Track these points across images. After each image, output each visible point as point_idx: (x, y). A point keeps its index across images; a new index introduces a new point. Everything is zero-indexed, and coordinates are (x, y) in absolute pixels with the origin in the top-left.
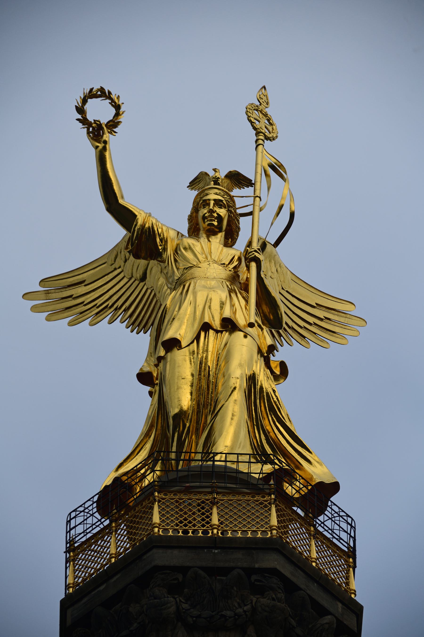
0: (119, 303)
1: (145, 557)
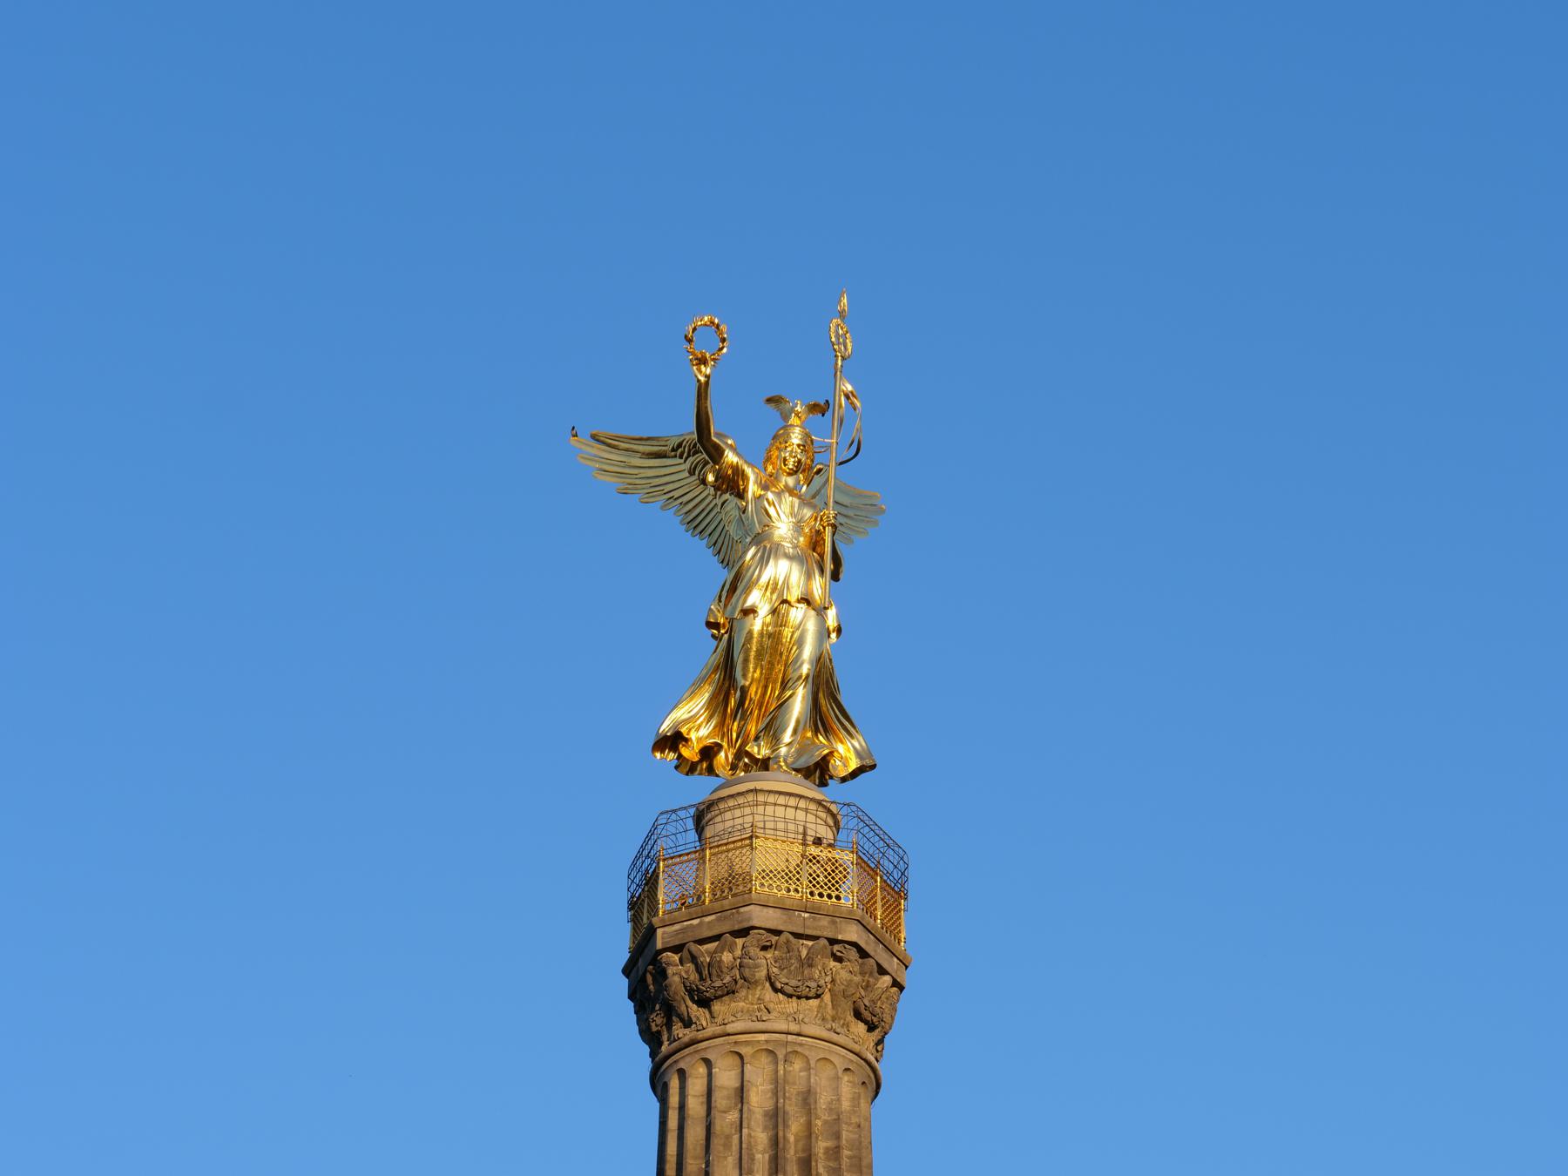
0: (676, 494)
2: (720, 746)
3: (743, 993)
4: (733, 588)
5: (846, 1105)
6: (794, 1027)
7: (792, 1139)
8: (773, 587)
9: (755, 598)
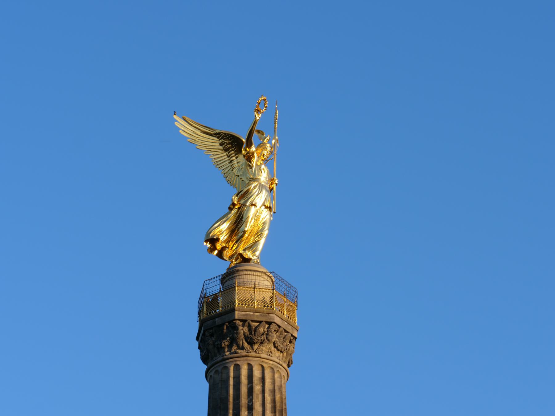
3: (266, 344)
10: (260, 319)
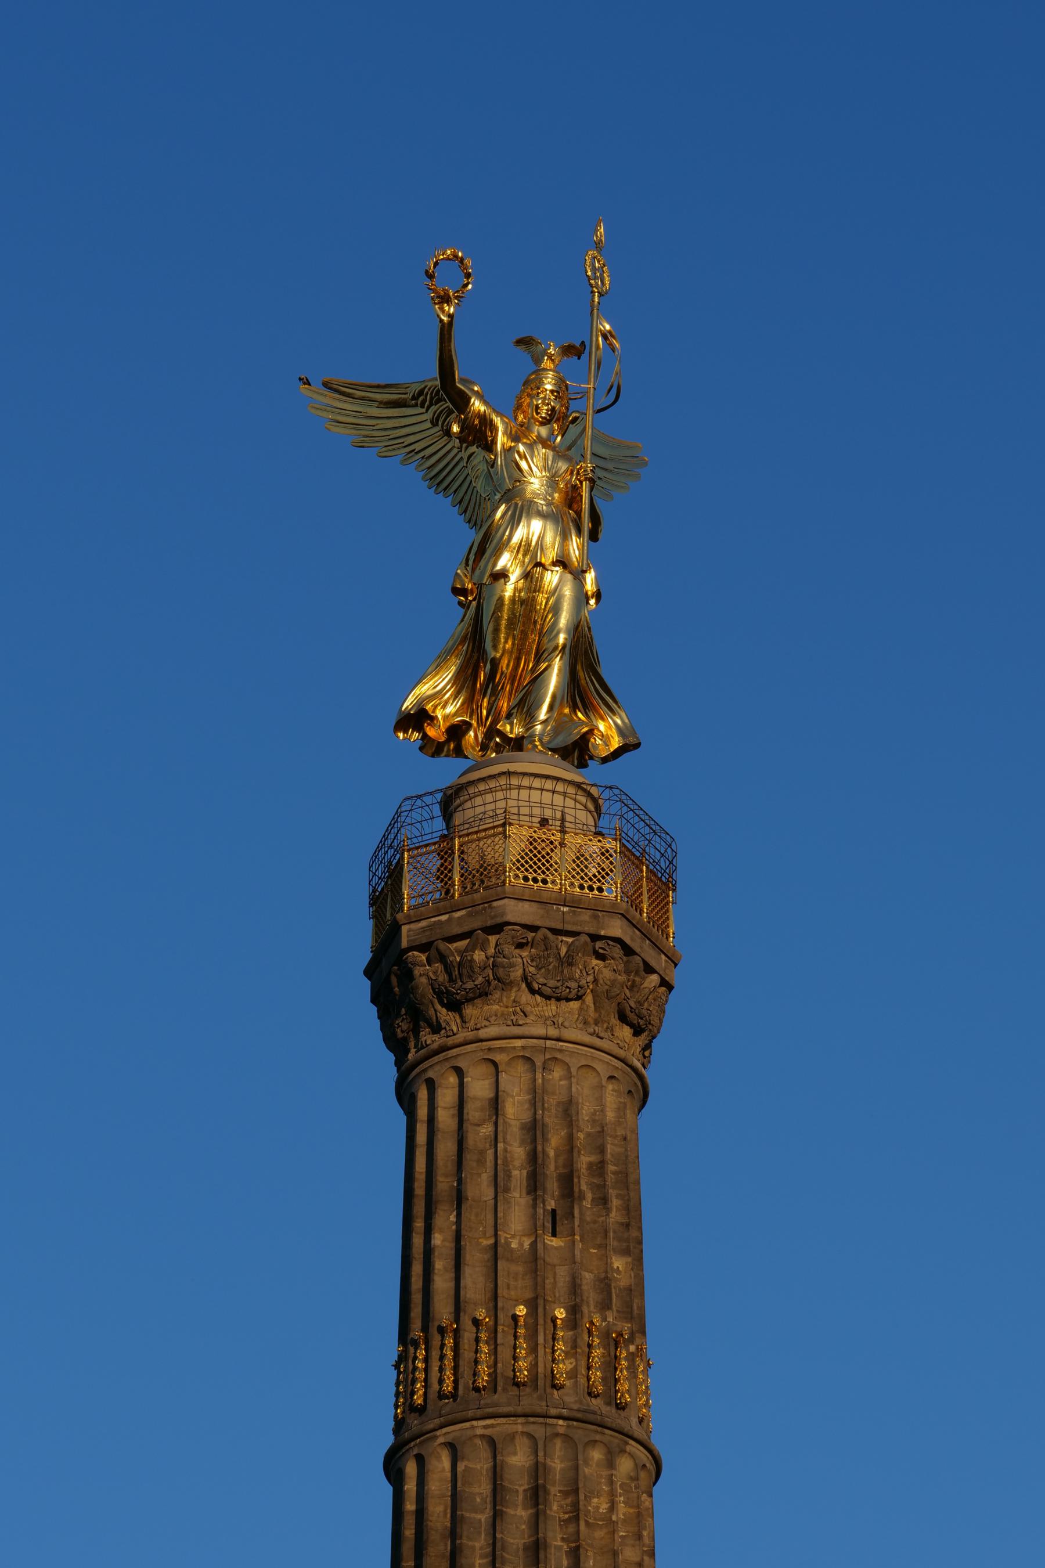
1: (495, 904)
2: (468, 725)
3: (497, 995)
4: (481, 551)
5: (610, 1115)
6: (553, 1032)
7: (552, 1153)
8: (525, 547)
9: (505, 560)
10: (466, 928)
